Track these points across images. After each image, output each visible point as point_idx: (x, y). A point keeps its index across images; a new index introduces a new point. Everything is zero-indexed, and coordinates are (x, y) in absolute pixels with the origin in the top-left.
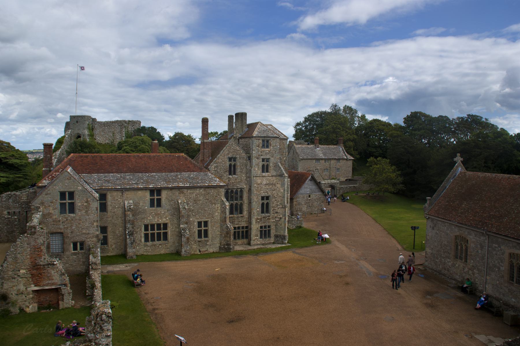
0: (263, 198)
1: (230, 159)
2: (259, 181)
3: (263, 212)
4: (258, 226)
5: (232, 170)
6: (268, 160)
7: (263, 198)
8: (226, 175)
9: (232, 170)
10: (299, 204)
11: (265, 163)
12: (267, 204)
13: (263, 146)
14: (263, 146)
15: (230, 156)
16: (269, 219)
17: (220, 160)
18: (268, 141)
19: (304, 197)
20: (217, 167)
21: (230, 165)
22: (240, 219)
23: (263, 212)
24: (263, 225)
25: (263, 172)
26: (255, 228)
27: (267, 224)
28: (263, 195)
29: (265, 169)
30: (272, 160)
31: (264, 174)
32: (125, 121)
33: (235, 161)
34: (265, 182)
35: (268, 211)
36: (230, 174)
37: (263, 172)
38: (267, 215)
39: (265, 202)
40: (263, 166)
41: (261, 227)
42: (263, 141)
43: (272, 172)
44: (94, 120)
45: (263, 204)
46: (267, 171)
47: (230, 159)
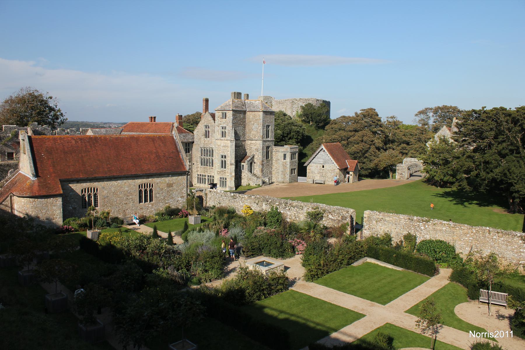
1: (206, 126)
3: (222, 167)
4: (219, 177)
7: (222, 157)
9: (207, 135)
10: (312, 172)
11: (223, 130)
12: (225, 161)
13: (223, 118)
14: (223, 117)
15: (205, 124)
16: (225, 173)
17: (200, 127)
19: (317, 167)
20: (198, 132)
21: (206, 131)
22: (211, 170)
24: (221, 177)
27: (224, 177)
29: (223, 134)
31: (222, 138)
33: (209, 128)
34: (222, 145)
35: (225, 168)
36: (206, 137)
37: (223, 136)
38: (224, 169)
39: (223, 159)
40: (223, 132)
41: (221, 178)
42: (223, 113)
43: (228, 137)
45: (222, 161)
47: (206, 126)
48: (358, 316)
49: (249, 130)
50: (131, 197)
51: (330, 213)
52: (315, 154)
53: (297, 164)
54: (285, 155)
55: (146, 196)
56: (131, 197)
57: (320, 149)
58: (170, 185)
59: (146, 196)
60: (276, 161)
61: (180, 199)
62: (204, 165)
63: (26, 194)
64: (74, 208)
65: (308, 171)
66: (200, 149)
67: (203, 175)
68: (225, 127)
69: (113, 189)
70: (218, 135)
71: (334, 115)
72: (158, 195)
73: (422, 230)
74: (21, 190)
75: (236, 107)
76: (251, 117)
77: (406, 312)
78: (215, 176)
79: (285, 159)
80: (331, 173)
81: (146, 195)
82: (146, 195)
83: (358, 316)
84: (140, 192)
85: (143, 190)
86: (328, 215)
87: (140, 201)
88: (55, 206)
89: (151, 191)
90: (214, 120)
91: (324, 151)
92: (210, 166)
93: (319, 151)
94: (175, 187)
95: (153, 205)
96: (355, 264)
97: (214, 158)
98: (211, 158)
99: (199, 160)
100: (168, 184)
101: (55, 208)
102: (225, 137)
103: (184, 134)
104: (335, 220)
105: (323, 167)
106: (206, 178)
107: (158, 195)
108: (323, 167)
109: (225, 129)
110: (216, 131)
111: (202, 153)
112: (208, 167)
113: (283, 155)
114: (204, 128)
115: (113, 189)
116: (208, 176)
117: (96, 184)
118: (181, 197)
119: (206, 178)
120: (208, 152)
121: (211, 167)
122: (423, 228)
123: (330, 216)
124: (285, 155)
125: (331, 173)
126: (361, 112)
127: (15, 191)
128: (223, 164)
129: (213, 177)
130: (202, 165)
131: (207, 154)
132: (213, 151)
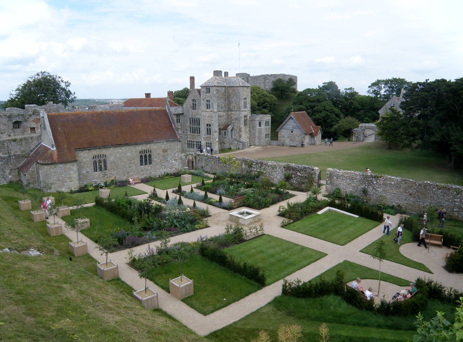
0: (207, 125)
1: (193, 100)
2: (204, 114)
3: (208, 134)
5: (194, 107)
6: (209, 100)
7: (207, 125)
8: (191, 110)
9: (194, 107)
10: (283, 137)
12: (210, 129)
13: (207, 93)
15: (192, 98)
18: (209, 89)
19: (287, 132)
20: (186, 105)
21: (193, 104)
23: (208, 134)
25: (207, 108)
26: (203, 143)
28: (207, 123)
29: (208, 106)
30: (211, 100)
32: (268, 75)
35: (210, 134)
36: (194, 109)
37: (207, 108)
38: (209, 136)
39: (209, 127)
40: (207, 105)
41: (207, 143)
44: (249, 75)
45: (208, 129)
46: (210, 108)
47: (193, 100)
48: (322, 255)
49: (229, 102)
50: (133, 161)
51: (298, 170)
52: (285, 121)
53: (270, 130)
54: (260, 123)
55: (146, 161)
56: (133, 161)
57: (289, 117)
58: (165, 151)
59: (146, 161)
60: (253, 127)
61: (173, 162)
62: (193, 133)
63: (48, 162)
64: (88, 172)
65: (279, 136)
66: (188, 120)
67: (192, 141)
68: (209, 100)
69: (118, 156)
70: (203, 107)
71: (301, 87)
72: (155, 159)
73: (374, 184)
74: (44, 159)
75: (218, 83)
76: (231, 91)
77: (327, 255)
78: (202, 142)
79: (260, 126)
80: (299, 137)
81: (146, 159)
82: (146, 159)
83: (322, 255)
84: (141, 157)
85: (143, 155)
86: (296, 173)
87: (141, 164)
88: (71, 171)
89: (150, 156)
90: (200, 94)
91: (293, 119)
92: (197, 133)
93: (288, 118)
94: (169, 152)
95: (151, 167)
96: (320, 213)
97: (200, 127)
98: (198, 126)
99: (188, 129)
100: (163, 150)
101: (71, 172)
102: (210, 108)
103: (175, 107)
104: (302, 177)
105: (292, 132)
106: (195, 143)
107: (155, 159)
108: (292, 132)
109: (209, 102)
110: (201, 104)
111: (190, 123)
112: (196, 134)
113: (258, 123)
114: (191, 102)
115: (118, 156)
116: (196, 142)
117: (104, 152)
118: (174, 160)
119: (195, 143)
120: (196, 121)
121: (198, 134)
122: (375, 182)
123: (299, 174)
124: (260, 123)
125: (299, 137)
126: (323, 85)
127: (39, 159)
128: (209, 132)
129: (200, 142)
130: (190, 133)
131: (195, 123)
132: (199, 120)
